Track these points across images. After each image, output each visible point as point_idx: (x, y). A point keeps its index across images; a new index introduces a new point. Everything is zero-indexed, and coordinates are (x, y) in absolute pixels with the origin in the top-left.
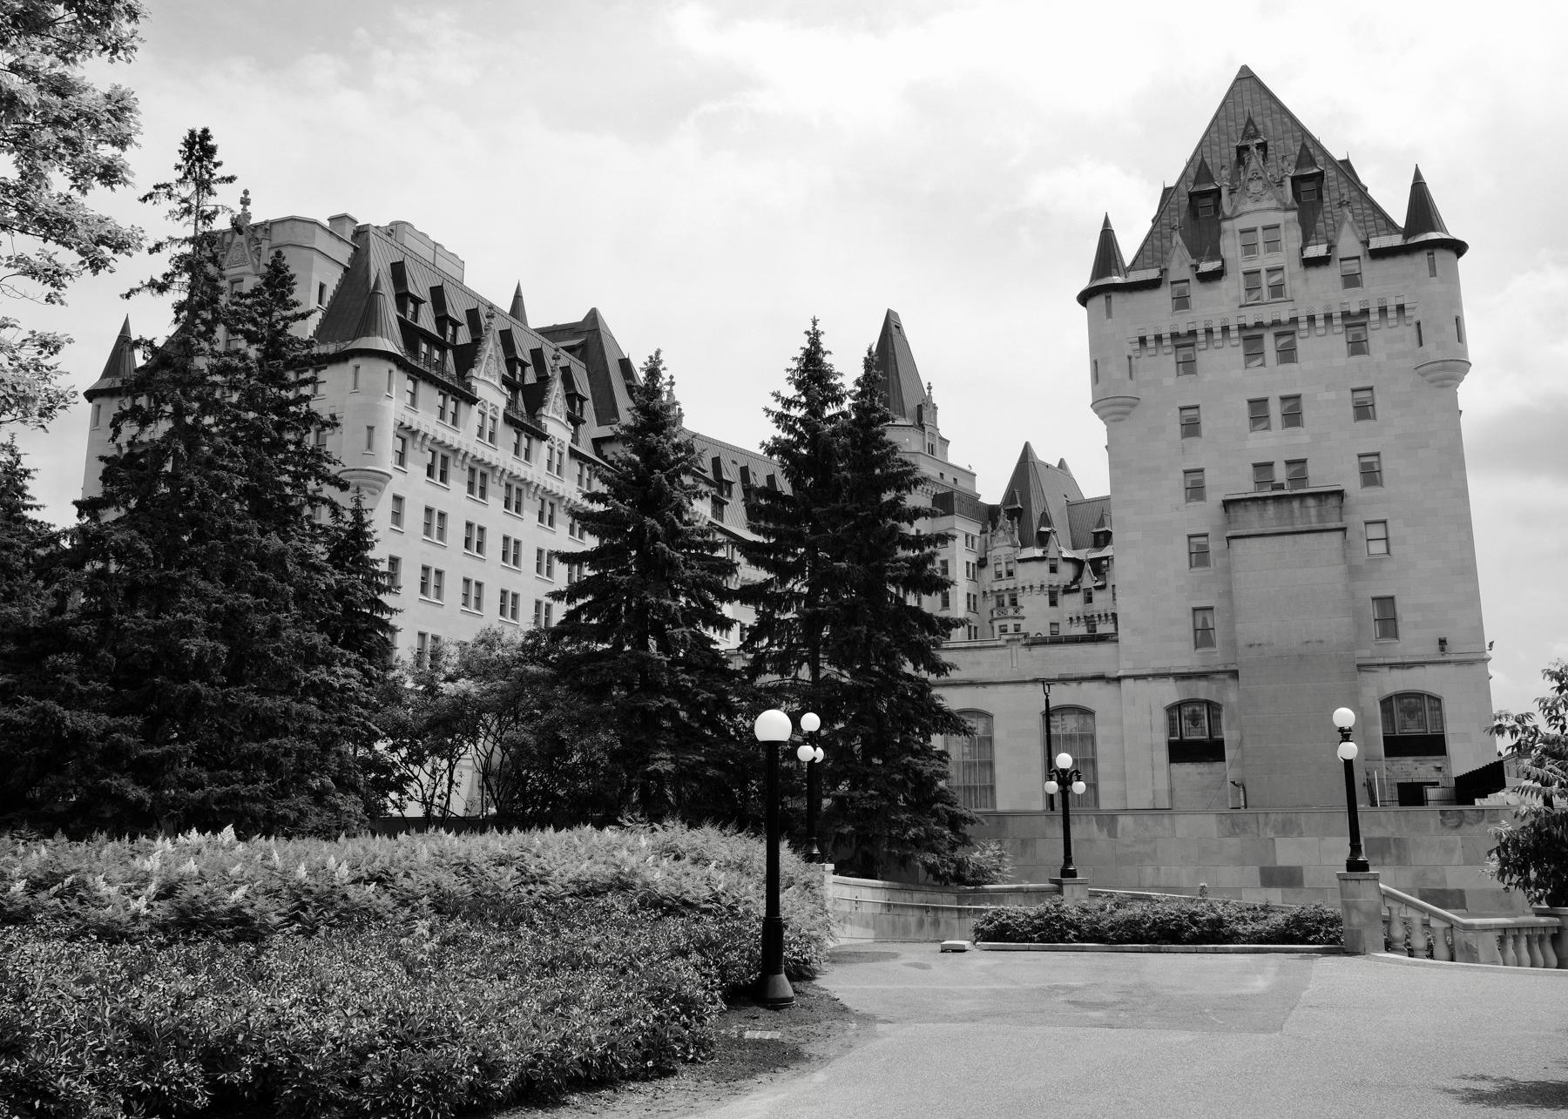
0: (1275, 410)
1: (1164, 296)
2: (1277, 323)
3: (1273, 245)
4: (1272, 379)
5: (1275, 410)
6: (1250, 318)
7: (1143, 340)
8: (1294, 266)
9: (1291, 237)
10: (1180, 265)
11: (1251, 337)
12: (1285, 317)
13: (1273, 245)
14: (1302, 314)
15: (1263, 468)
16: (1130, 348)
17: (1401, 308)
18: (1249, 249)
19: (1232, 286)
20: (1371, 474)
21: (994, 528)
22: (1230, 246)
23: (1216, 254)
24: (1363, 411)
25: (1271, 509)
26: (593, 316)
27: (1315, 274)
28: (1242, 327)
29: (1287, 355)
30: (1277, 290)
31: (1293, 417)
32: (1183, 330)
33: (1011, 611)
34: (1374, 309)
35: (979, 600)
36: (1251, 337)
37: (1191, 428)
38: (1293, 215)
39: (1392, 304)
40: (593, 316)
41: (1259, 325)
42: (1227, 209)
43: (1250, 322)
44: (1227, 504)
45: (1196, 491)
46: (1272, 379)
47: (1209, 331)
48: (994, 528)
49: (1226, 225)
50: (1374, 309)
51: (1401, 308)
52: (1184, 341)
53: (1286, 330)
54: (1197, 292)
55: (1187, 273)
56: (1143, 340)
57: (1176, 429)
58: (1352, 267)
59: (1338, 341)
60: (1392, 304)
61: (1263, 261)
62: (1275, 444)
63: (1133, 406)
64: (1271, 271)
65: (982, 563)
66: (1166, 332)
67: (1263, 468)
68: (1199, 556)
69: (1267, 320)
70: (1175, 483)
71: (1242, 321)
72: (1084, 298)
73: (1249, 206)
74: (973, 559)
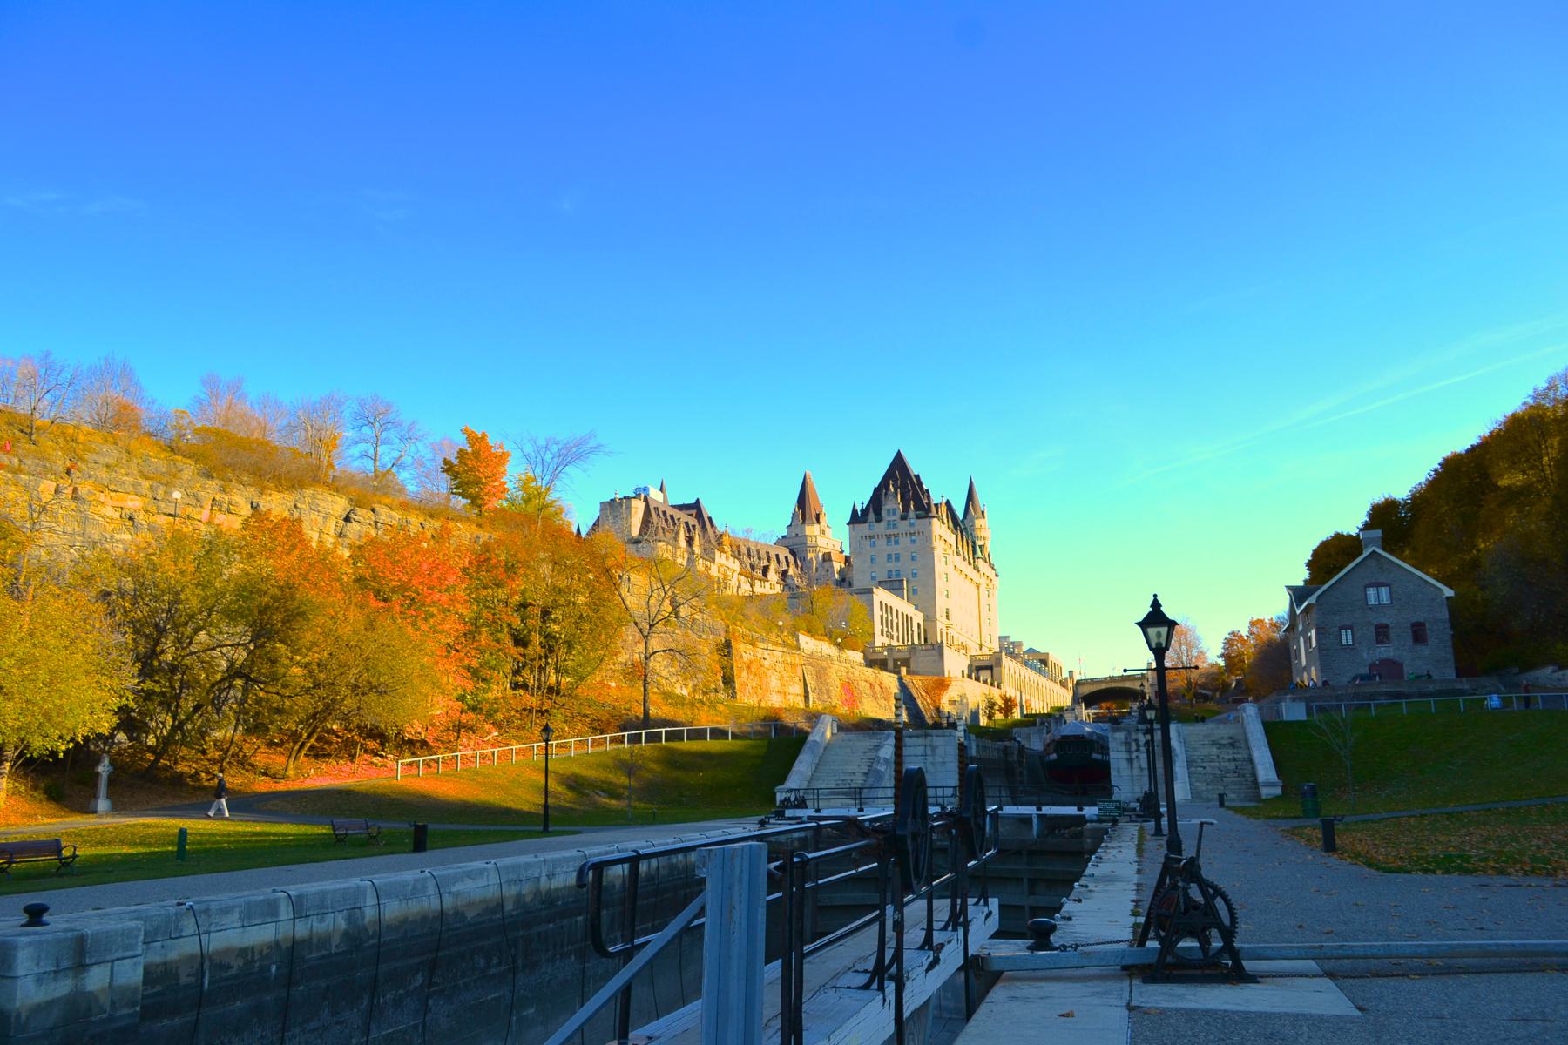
0: (893, 557)
1: (866, 526)
3: (894, 514)
4: (893, 549)
5: (893, 557)
6: (888, 532)
8: (899, 521)
10: (872, 516)
11: (888, 537)
13: (894, 514)
19: (883, 524)
22: (884, 513)
23: (880, 514)
24: (913, 558)
26: (698, 500)
27: (903, 522)
29: (897, 543)
30: (895, 526)
31: (897, 559)
32: (872, 535)
37: (872, 560)
40: (698, 500)
46: (893, 549)
49: (883, 507)
53: (896, 536)
54: (876, 525)
55: (874, 520)
58: (912, 521)
62: (892, 566)
72: (848, 524)
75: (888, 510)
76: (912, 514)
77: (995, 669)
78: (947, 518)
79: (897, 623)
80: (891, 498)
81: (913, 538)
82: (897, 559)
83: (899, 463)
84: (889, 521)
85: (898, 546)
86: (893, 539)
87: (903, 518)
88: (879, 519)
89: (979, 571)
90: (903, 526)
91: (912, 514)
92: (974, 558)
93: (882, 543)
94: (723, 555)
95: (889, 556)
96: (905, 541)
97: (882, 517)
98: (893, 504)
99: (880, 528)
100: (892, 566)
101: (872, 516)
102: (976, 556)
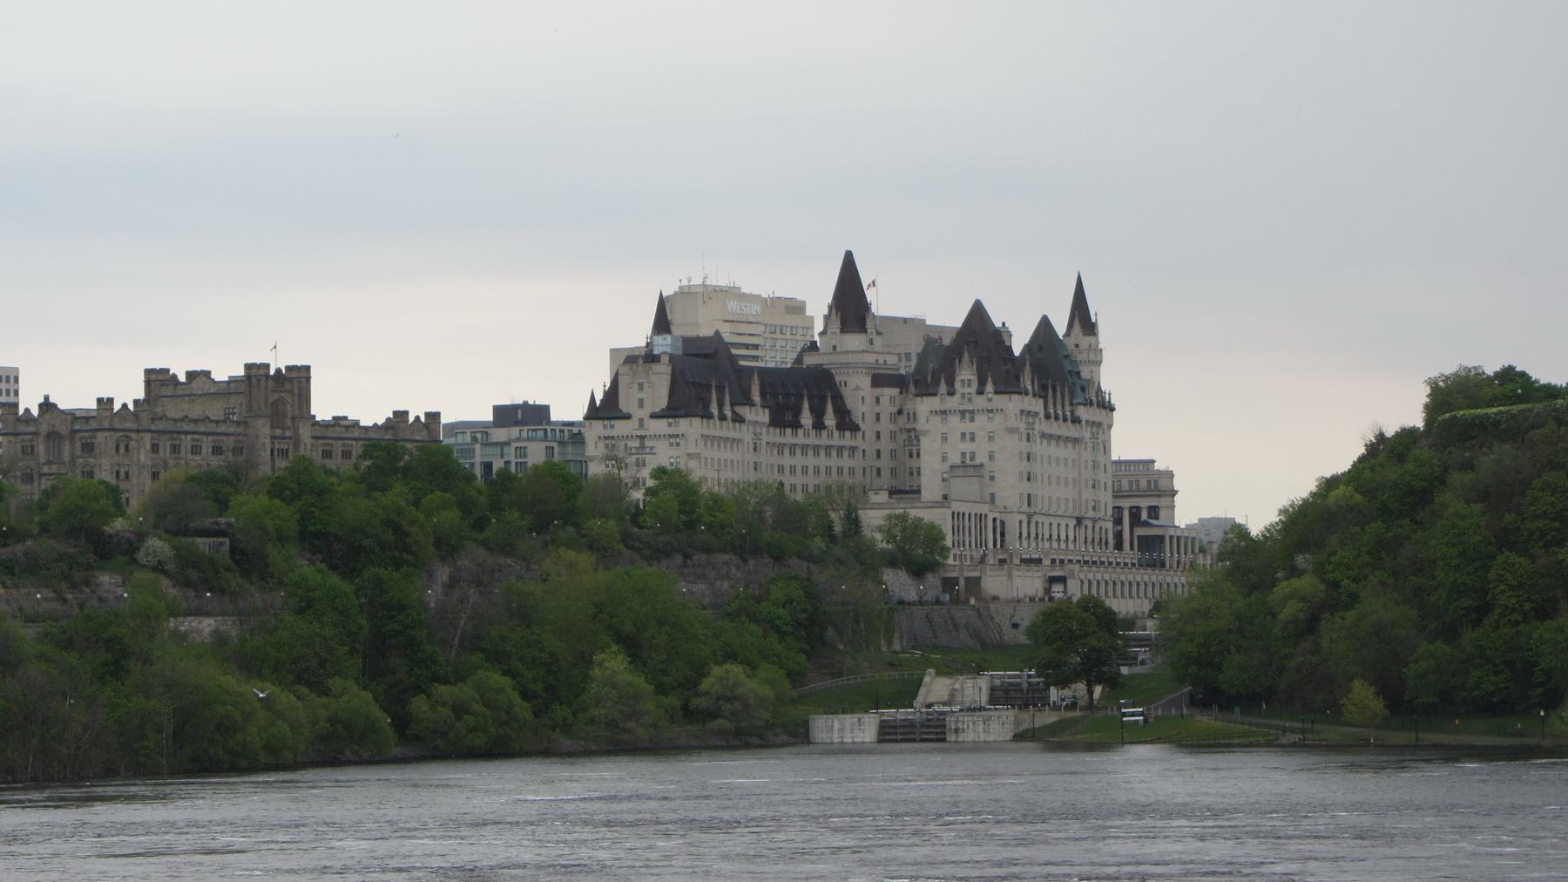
0: (968, 436)
2: (968, 410)
3: (969, 386)
5: (968, 436)
6: (962, 408)
7: (932, 412)
8: (974, 394)
9: (975, 385)
10: (943, 388)
13: (969, 386)
15: (963, 454)
16: (927, 414)
18: (963, 385)
19: (956, 399)
20: (991, 457)
21: (906, 392)
22: (958, 385)
24: (991, 438)
25: (961, 469)
27: (981, 397)
28: (959, 411)
29: (972, 420)
30: (970, 400)
31: (972, 439)
33: (915, 442)
35: (898, 434)
36: (963, 413)
37: (944, 439)
38: (976, 377)
39: (1000, 408)
42: (957, 372)
44: (951, 467)
45: (944, 459)
46: (968, 427)
47: (950, 411)
48: (906, 392)
52: (944, 412)
53: (972, 412)
54: (949, 399)
55: (946, 392)
56: (932, 412)
57: (940, 440)
58: (990, 396)
60: (1000, 408)
61: (967, 390)
62: (967, 447)
64: (969, 394)
65: (900, 412)
66: (938, 410)
67: (963, 454)
68: (944, 480)
70: (939, 457)
73: (963, 373)
74: (894, 410)
75: (963, 381)
76: (989, 387)
77: (1069, 581)
78: (1033, 382)
79: (970, 528)
80: (966, 366)
81: (991, 415)
82: (972, 439)
83: (978, 313)
84: (963, 394)
85: (972, 424)
86: (967, 415)
87: (980, 392)
88: (951, 394)
89: (1079, 421)
90: (980, 402)
91: (989, 387)
92: (1071, 404)
93: (954, 420)
94: (753, 409)
95: (963, 435)
96: (981, 419)
97: (955, 390)
98: (966, 374)
99: (953, 403)
100: (967, 447)
101: (943, 388)
102: (1075, 401)
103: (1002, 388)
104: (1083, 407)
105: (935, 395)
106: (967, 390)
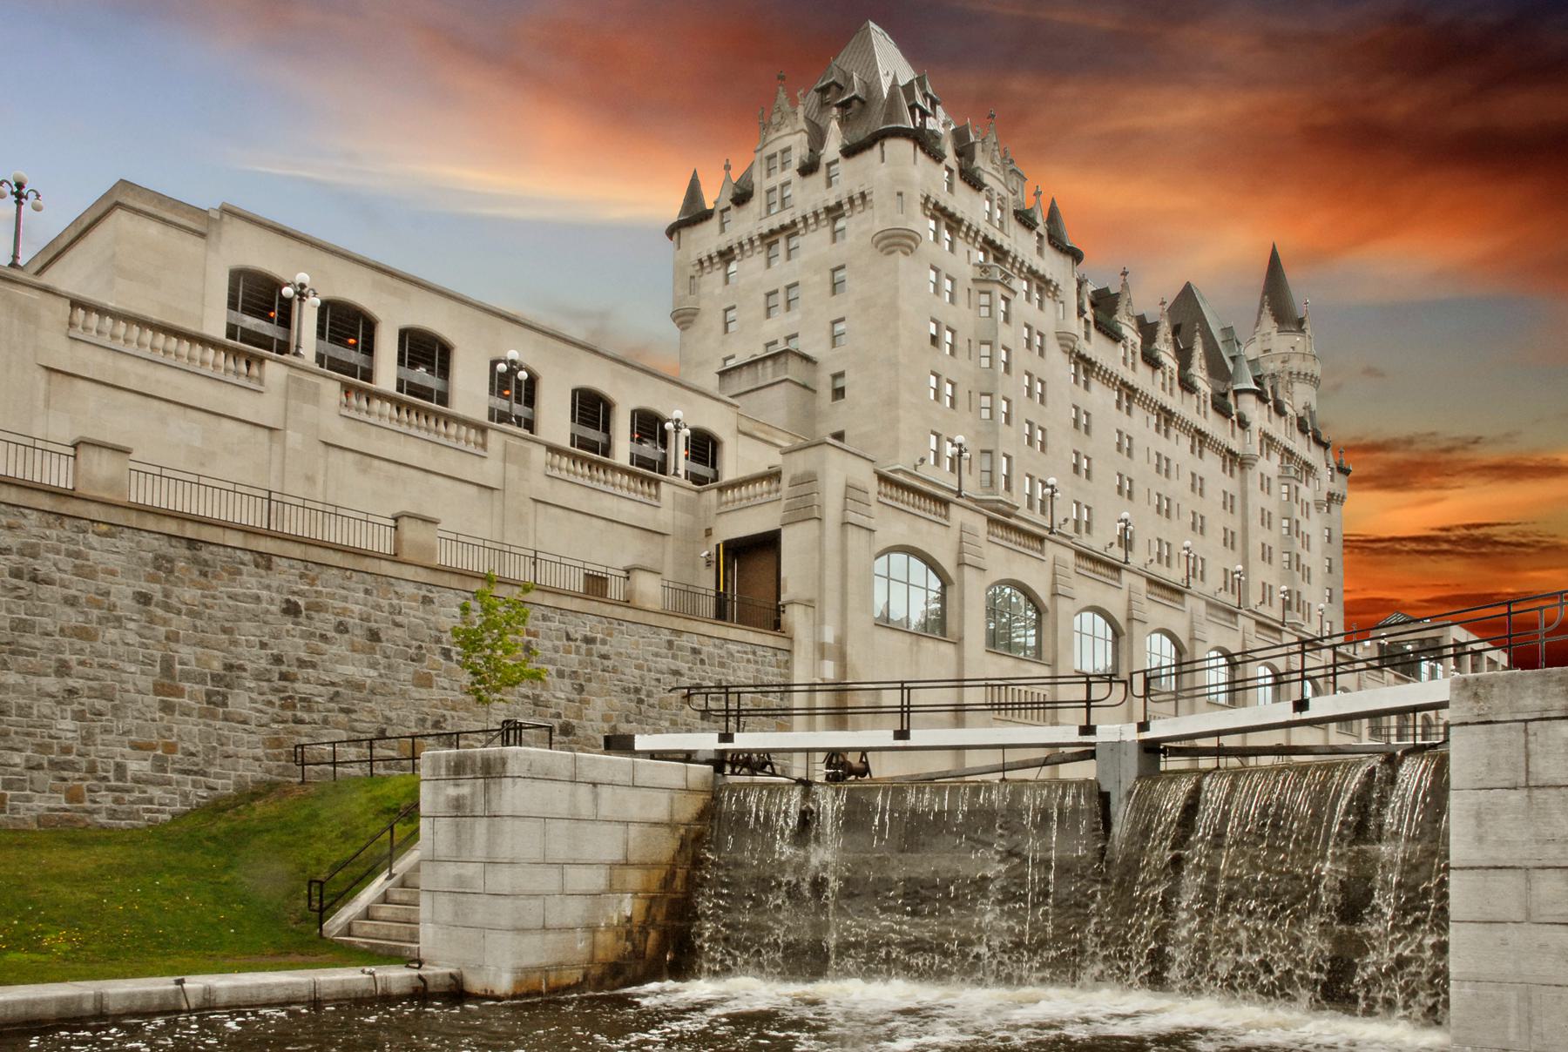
2: (783, 228)
12: (787, 221)
14: (798, 217)
16: (691, 271)
17: (863, 196)
34: (845, 200)
39: (856, 195)
41: (772, 232)
43: (765, 230)
47: (741, 245)
50: (845, 200)
51: (863, 196)
52: (726, 256)
53: (789, 230)
56: (701, 262)
59: (825, 232)
61: (778, 178)
63: (695, 315)
64: (788, 183)
66: (714, 253)
69: (776, 226)
71: (760, 231)
87: (808, 169)
96: (814, 243)
99: (748, 222)
103: (861, 133)
104: (1252, 398)
105: (706, 215)
106: (778, 178)
